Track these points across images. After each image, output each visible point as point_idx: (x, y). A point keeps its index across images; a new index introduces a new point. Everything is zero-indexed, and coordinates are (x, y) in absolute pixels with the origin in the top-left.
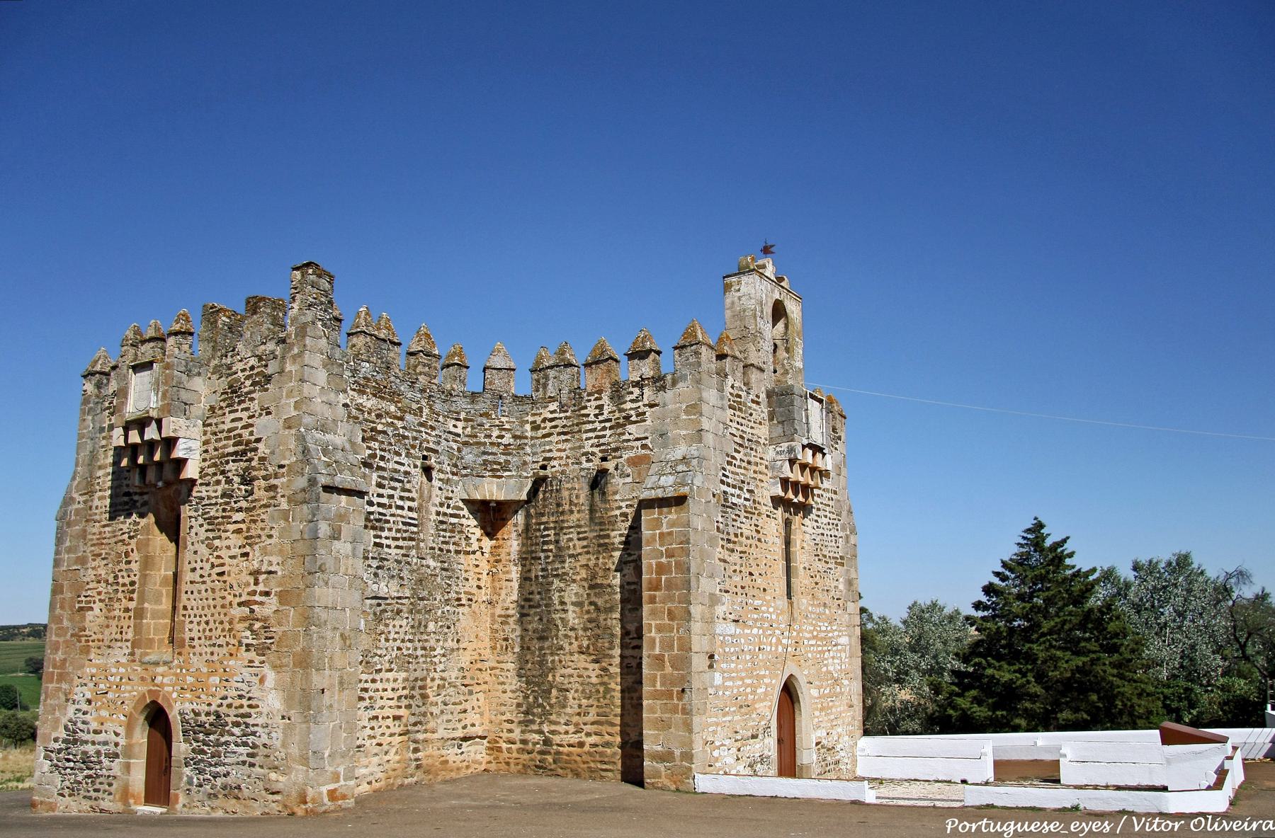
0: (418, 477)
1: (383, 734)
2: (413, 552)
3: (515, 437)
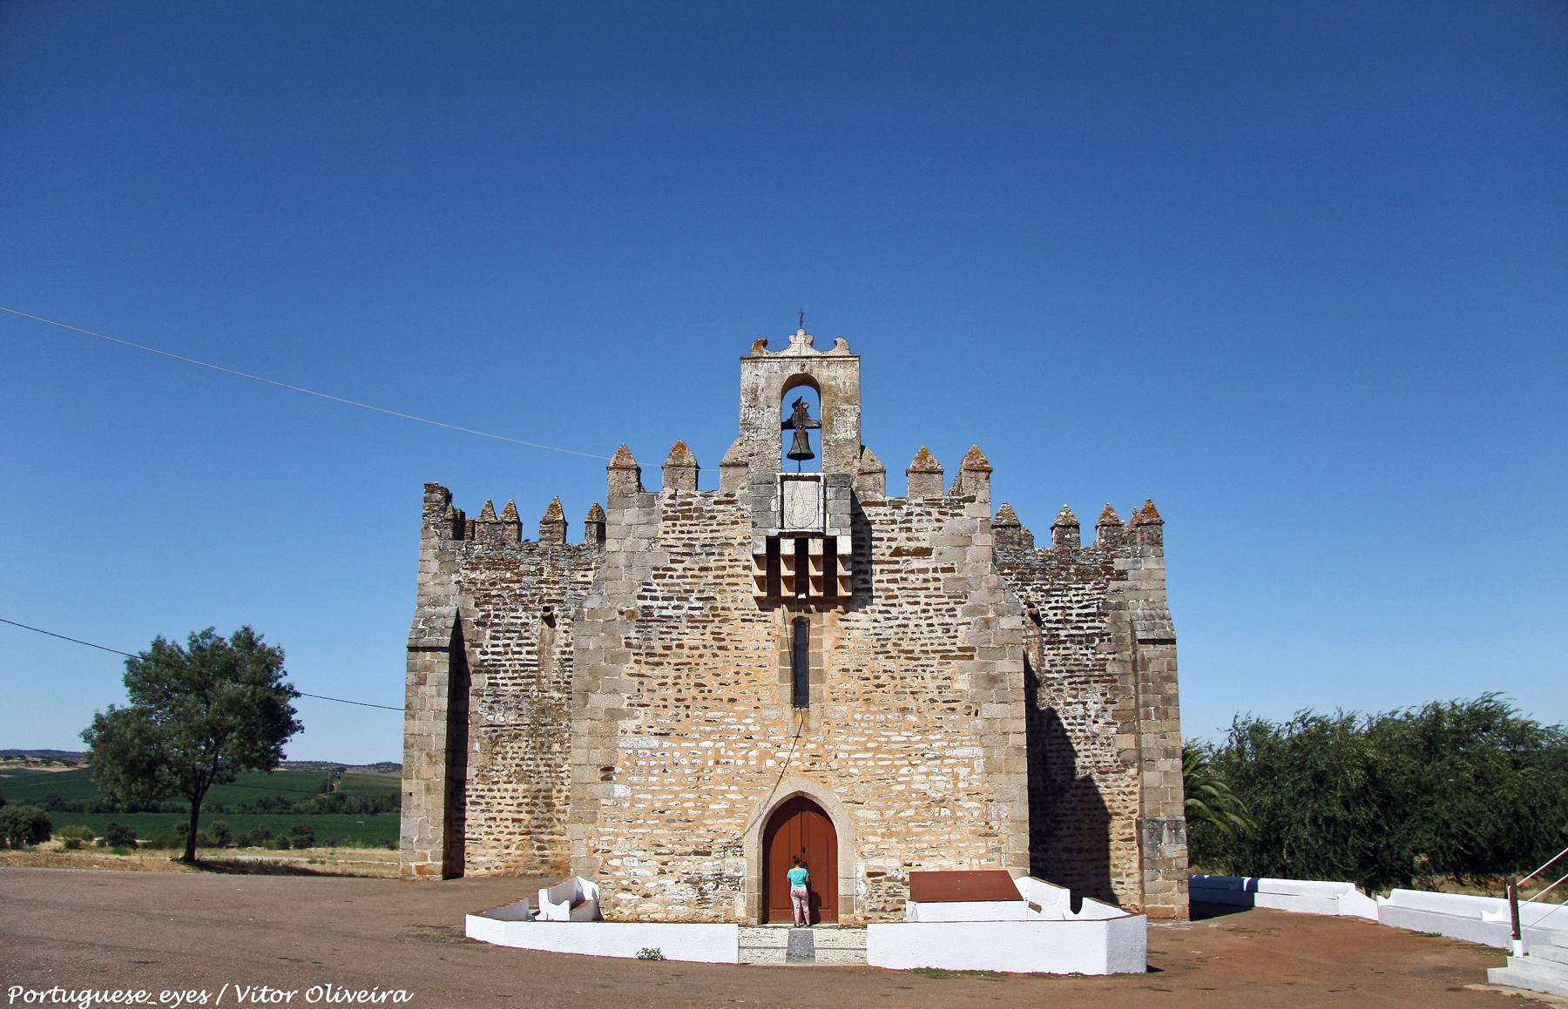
0: (538, 626)
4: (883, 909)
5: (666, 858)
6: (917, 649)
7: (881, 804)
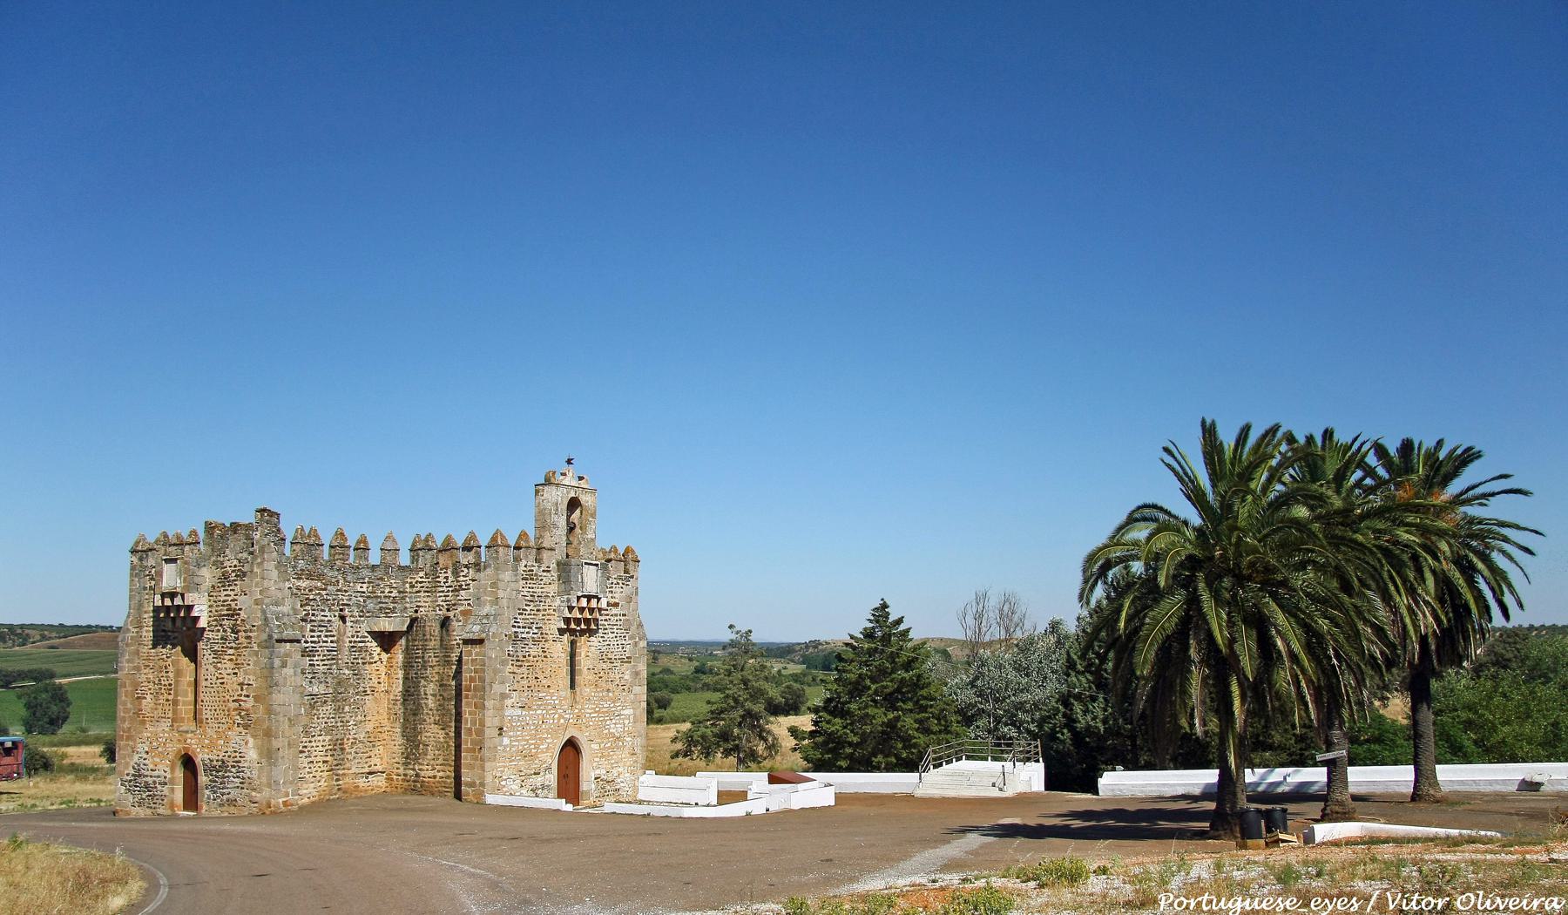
0: (337, 622)
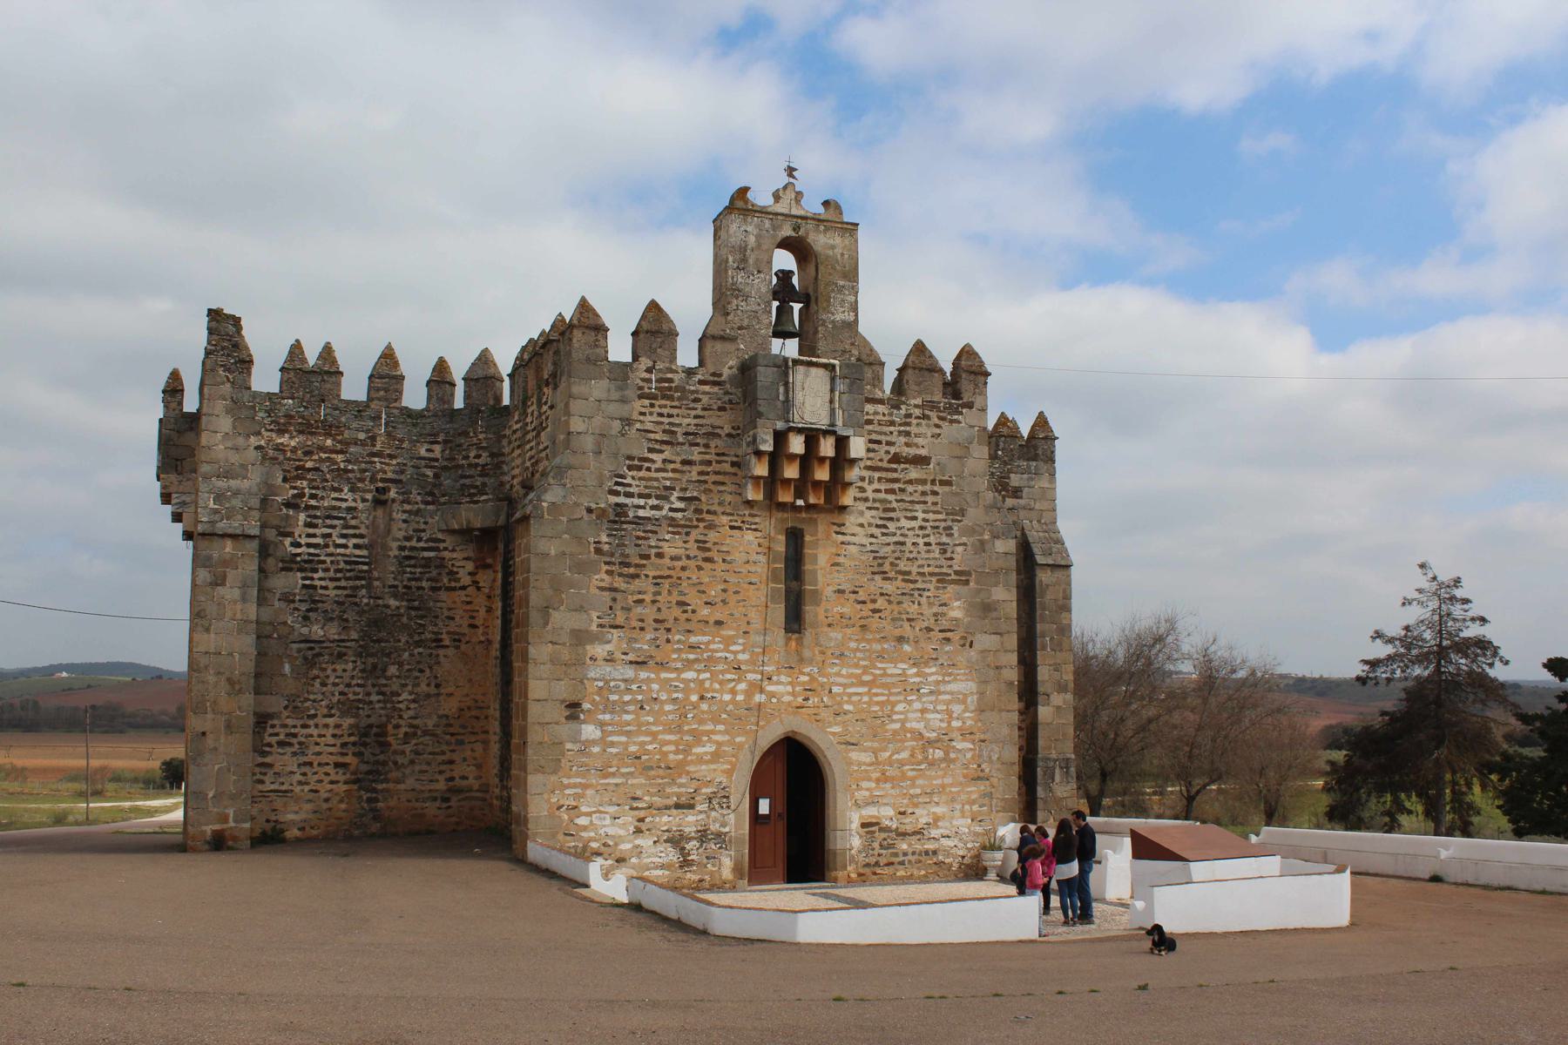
1: (321, 781)
2: (364, 591)
3: (492, 455)
4: (877, 864)
5: (642, 814)
6: (914, 570)
7: (876, 745)
